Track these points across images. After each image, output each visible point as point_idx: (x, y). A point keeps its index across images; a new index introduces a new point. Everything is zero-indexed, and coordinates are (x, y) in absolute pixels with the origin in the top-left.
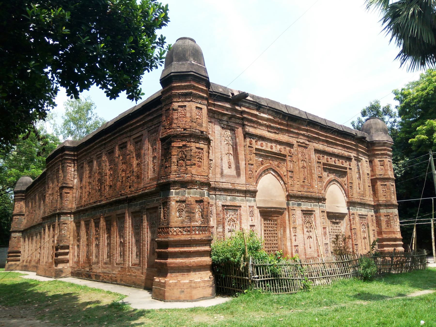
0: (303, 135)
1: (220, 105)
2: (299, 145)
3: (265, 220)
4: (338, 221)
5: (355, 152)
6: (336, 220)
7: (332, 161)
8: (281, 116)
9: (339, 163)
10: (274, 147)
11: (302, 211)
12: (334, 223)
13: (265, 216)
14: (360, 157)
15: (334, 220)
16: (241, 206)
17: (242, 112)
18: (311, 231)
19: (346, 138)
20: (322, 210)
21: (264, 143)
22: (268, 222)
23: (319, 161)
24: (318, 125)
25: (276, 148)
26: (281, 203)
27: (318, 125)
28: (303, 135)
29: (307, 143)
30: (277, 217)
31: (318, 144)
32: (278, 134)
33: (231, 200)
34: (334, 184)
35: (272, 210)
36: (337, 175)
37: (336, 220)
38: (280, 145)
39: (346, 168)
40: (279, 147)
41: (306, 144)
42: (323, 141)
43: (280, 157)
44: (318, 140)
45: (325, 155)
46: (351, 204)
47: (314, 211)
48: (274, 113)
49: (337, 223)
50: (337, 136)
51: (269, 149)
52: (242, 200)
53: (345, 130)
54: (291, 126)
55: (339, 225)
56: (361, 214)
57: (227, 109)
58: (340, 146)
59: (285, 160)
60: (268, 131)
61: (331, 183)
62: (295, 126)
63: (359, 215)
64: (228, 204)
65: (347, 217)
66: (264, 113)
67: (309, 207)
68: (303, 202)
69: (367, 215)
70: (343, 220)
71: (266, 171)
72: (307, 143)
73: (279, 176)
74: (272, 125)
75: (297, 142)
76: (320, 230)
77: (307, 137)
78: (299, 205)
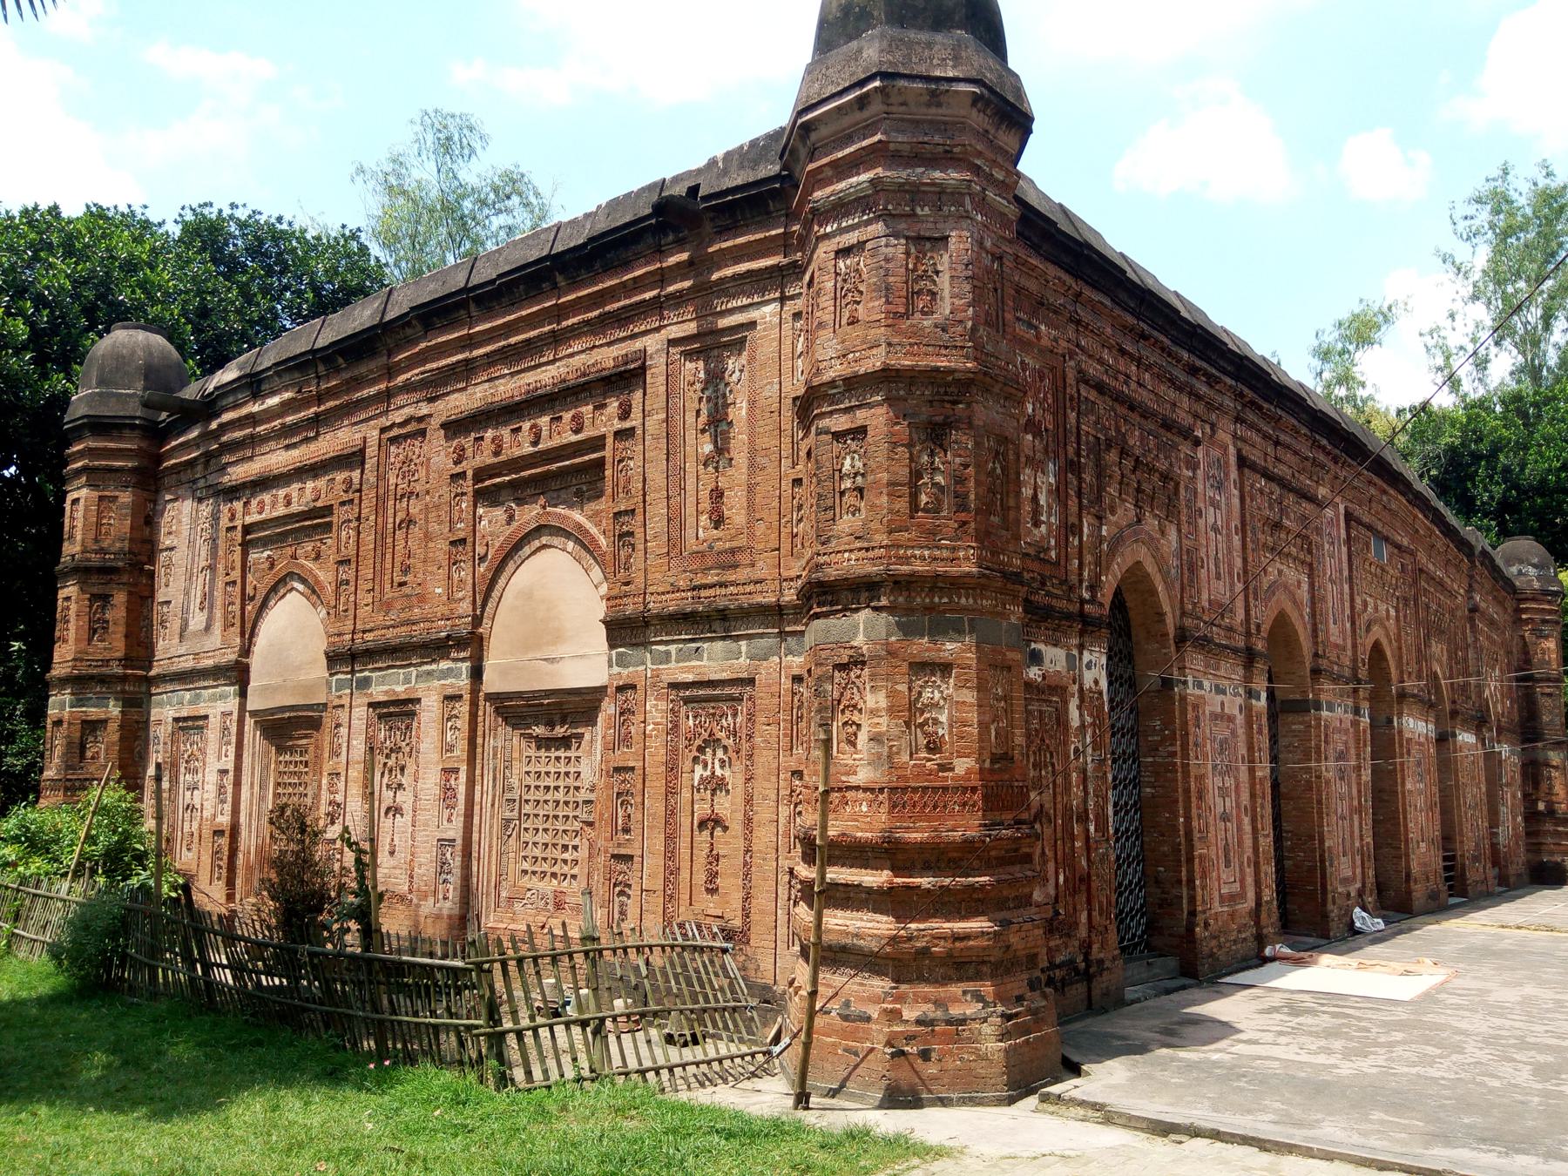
0: (408, 387)
1: (181, 445)
2: (393, 440)
3: (281, 750)
4: (560, 731)
5: (689, 312)
6: (551, 724)
7: (518, 442)
8: (321, 368)
9: (556, 432)
10: (295, 495)
11: (370, 705)
12: (544, 743)
13: (281, 736)
14: (724, 322)
15: (539, 730)
16: (206, 717)
17: (223, 428)
18: (400, 786)
19: (627, 265)
20: (450, 692)
21: (266, 497)
22: (288, 758)
23: (458, 469)
24: (463, 305)
25: (302, 495)
26: (309, 688)
27: (463, 305)
28: (408, 387)
29: (424, 409)
30: (306, 737)
31: (470, 390)
32: (315, 438)
33: (190, 703)
34: (544, 547)
35: (287, 715)
36: (563, 495)
37: (551, 724)
38: (316, 477)
39: (598, 443)
40: (310, 485)
41: (421, 419)
42: (492, 360)
43: (315, 521)
44: (466, 371)
45: (485, 429)
46: (625, 630)
47: (418, 700)
48: (297, 375)
49: (565, 742)
50: (575, 285)
51: (281, 511)
52: (213, 699)
53: (602, 226)
54: (358, 383)
55: (572, 754)
56: (690, 678)
57: (194, 444)
58: (578, 336)
59: (328, 527)
60: (287, 447)
61: (527, 550)
62: (371, 371)
63: (674, 686)
64: (184, 714)
65: (608, 708)
66: (273, 393)
67: (400, 688)
68: (380, 669)
69: (751, 681)
70: (592, 722)
71: (277, 588)
72: (424, 409)
73: (314, 591)
74: (289, 419)
75: (383, 430)
76: (431, 781)
77: (424, 384)
78: (365, 683)
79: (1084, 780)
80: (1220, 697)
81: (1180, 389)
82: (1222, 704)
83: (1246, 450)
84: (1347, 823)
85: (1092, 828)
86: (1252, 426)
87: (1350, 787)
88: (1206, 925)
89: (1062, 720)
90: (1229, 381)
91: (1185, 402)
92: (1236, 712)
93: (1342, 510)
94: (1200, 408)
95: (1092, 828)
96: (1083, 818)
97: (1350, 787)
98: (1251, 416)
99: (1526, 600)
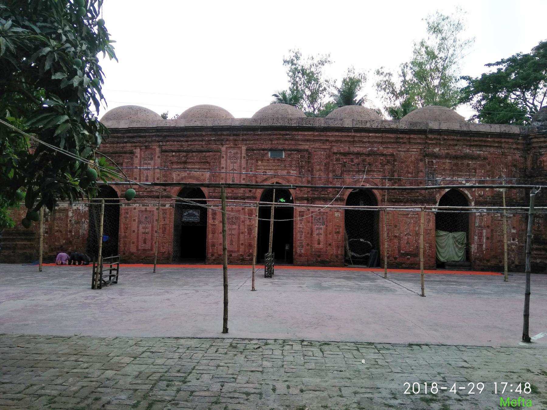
79: (72, 225)
80: (144, 207)
81: (126, 143)
82: (146, 208)
83: (164, 148)
84: (236, 236)
85: (73, 234)
86: (168, 141)
87: (239, 226)
88: (124, 254)
89: (67, 216)
90: (153, 134)
91: (129, 145)
92: (155, 210)
93: (244, 148)
94: (137, 144)
95: (73, 234)
96: (71, 232)
97: (239, 226)
98: (169, 138)
99: (532, 138)
